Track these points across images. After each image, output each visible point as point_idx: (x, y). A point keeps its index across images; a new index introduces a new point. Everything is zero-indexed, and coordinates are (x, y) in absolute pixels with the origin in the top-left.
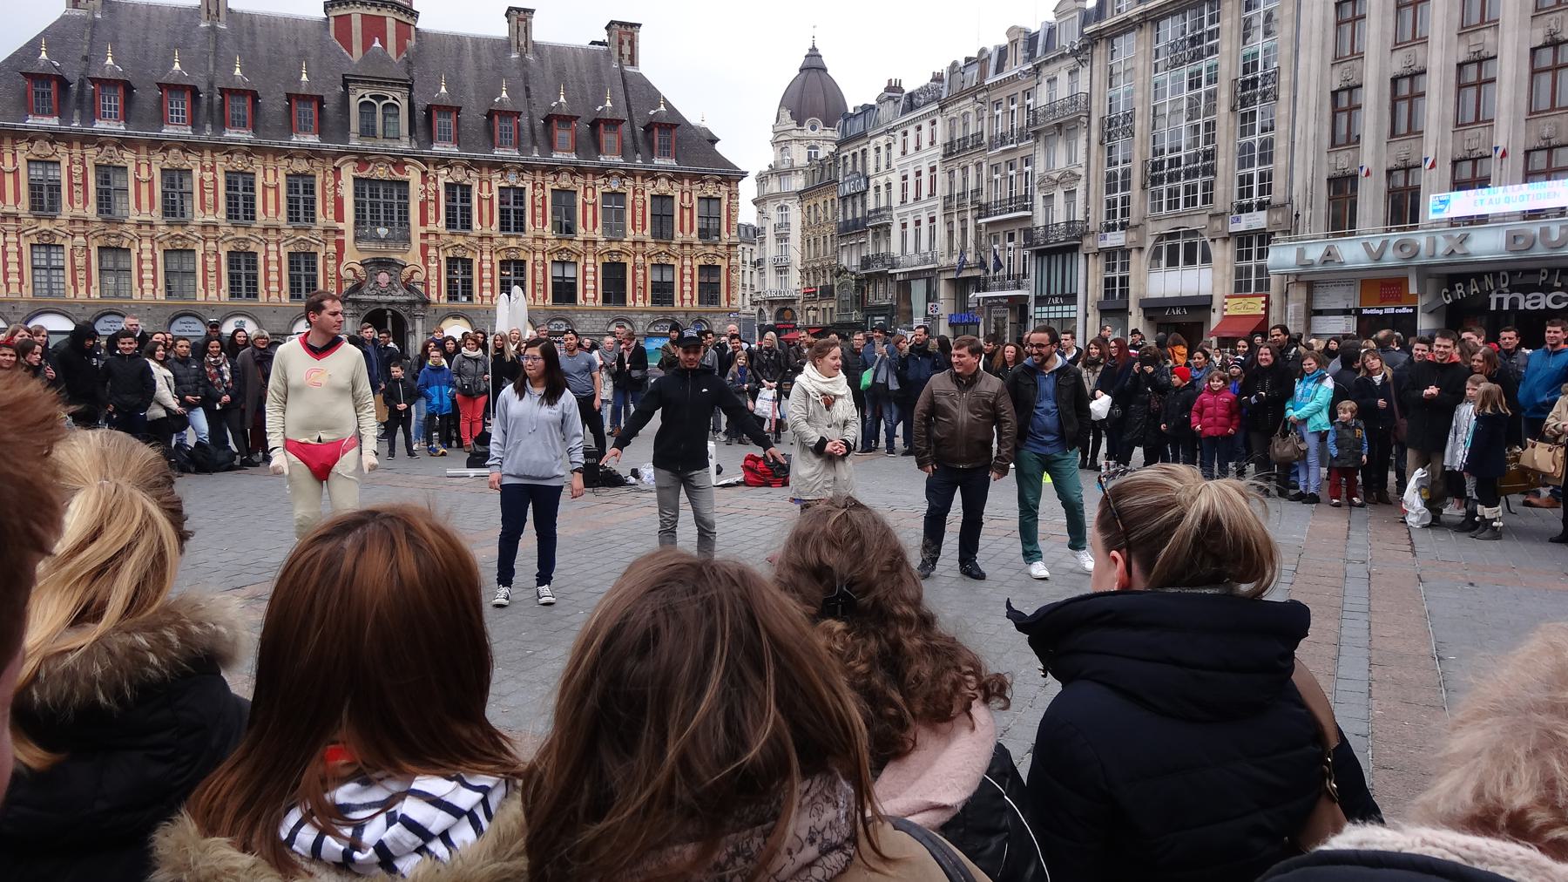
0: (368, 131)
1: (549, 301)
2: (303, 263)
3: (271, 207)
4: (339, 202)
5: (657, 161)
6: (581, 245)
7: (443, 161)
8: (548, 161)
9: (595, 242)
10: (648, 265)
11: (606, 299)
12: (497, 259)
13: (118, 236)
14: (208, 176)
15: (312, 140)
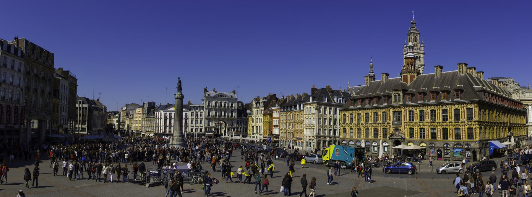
0: (396, 101)
1: (430, 138)
2: (384, 130)
3: (380, 120)
4: (390, 117)
5: (455, 100)
7: (407, 106)
8: (429, 103)
11: (444, 138)
12: (418, 128)
15: (386, 104)
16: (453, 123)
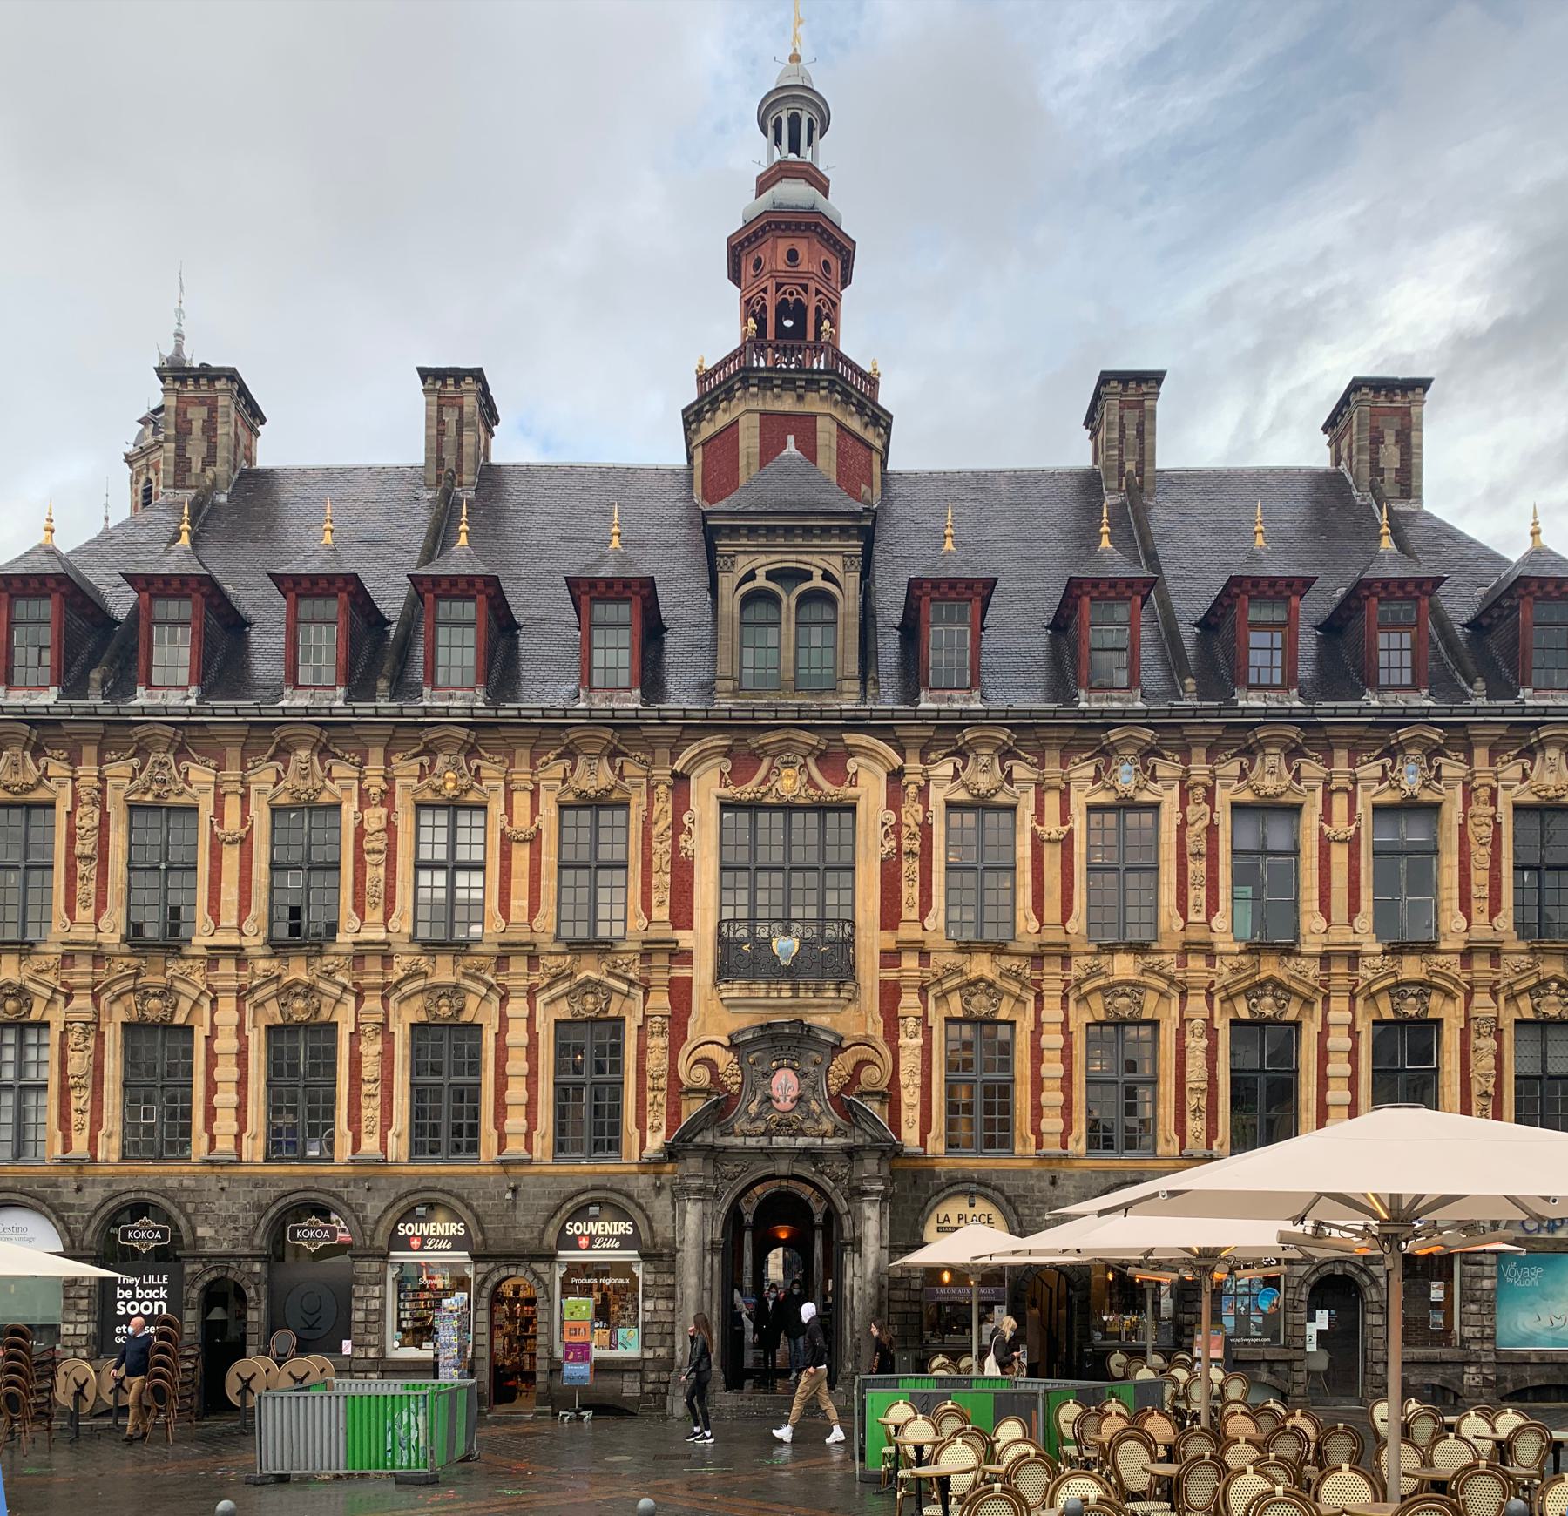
6: (1313, 969)
9: (1354, 958)
10: (1507, 1022)
13: (167, 992)
14: (375, 817)
16: (1509, 963)
